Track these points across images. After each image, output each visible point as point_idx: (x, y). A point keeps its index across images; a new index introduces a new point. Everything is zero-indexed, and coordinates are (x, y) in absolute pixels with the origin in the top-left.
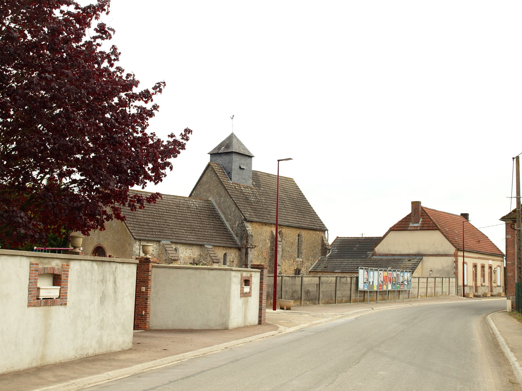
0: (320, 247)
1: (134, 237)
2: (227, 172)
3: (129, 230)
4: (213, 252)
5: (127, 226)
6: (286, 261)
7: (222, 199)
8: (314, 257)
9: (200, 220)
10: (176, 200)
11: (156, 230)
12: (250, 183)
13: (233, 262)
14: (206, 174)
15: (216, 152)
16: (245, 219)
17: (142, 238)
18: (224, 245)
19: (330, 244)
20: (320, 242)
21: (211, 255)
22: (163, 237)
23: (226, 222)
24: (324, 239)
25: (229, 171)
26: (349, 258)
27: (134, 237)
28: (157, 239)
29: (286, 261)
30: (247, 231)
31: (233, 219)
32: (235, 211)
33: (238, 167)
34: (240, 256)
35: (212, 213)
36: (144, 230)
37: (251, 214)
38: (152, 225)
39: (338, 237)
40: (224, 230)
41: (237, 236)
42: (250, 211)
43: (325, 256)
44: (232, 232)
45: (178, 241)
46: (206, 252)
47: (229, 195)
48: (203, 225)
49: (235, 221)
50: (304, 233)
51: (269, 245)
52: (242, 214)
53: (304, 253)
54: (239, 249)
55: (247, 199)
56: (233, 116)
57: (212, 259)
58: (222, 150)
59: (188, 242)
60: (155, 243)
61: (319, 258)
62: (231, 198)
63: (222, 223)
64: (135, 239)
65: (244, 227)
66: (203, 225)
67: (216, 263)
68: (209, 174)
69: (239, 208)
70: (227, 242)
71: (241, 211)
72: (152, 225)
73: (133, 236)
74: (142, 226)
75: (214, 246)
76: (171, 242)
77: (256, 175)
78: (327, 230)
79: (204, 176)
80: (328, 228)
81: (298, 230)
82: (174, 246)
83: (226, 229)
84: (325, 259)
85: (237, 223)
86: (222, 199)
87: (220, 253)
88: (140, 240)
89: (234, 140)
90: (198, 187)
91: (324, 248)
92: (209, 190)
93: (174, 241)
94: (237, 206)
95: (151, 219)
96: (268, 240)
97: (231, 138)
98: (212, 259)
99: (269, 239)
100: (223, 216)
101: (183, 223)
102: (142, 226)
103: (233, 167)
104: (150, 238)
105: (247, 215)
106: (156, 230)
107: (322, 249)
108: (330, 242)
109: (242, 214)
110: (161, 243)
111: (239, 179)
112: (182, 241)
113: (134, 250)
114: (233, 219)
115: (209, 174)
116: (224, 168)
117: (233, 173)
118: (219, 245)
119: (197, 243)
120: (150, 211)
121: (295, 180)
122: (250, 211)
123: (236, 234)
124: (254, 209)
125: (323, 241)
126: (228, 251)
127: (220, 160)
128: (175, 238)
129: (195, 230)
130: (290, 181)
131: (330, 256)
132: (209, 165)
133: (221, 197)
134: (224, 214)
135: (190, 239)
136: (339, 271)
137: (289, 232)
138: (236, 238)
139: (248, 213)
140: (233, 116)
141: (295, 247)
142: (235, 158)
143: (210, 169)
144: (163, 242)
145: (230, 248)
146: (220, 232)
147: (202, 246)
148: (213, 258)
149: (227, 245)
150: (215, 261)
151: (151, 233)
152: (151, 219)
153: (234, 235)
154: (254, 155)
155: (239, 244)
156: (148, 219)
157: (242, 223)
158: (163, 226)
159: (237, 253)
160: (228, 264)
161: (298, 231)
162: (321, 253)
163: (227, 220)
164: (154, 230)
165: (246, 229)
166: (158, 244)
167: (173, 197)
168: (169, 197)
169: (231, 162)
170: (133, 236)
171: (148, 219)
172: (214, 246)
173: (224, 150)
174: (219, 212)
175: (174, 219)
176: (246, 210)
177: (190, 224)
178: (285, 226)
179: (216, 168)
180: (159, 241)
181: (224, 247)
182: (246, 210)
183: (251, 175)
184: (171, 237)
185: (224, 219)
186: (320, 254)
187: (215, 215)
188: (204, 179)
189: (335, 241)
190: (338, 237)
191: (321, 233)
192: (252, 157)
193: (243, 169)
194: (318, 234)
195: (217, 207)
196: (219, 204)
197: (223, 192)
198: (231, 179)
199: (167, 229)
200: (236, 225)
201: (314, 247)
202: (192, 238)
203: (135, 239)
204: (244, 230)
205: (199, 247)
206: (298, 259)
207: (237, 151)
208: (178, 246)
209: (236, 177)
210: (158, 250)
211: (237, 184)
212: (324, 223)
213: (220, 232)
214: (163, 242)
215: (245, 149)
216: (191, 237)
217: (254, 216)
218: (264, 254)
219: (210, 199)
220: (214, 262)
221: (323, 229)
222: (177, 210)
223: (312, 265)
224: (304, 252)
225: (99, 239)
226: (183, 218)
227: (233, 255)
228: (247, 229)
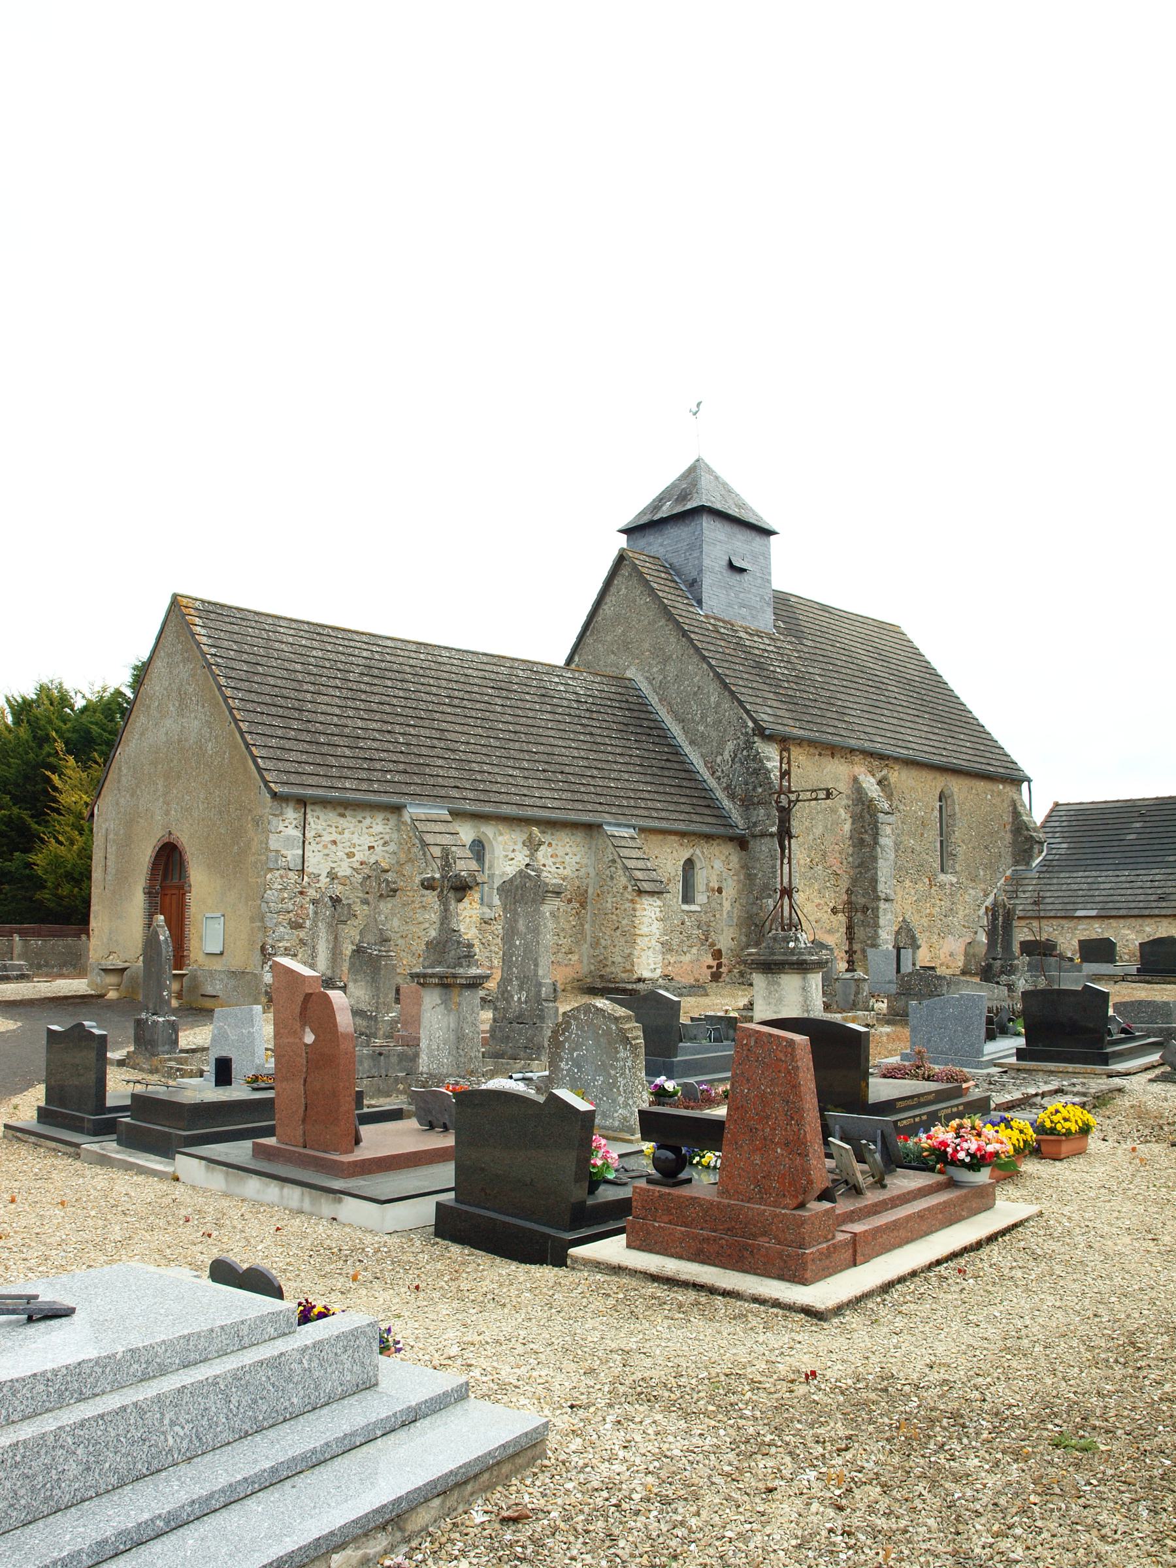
0: (1008, 837)
1: (269, 789)
2: (684, 582)
3: (254, 758)
4: (639, 854)
5: (247, 745)
6: (908, 883)
7: (672, 670)
8: (991, 867)
9: (588, 738)
10: (495, 669)
11: (391, 766)
12: (766, 621)
13: (720, 891)
14: (613, 590)
15: (645, 519)
16: (760, 732)
17: (310, 791)
18: (681, 827)
19: (1038, 824)
20: (1008, 818)
21: (631, 864)
22: (418, 790)
23: (688, 749)
24: (1020, 809)
25: (694, 574)
26: (1117, 867)
27: (269, 789)
28: (384, 798)
29: (908, 883)
30: (768, 771)
31: (714, 734)
32: (718, 705)
33: (725, 563)
34: (745, 867)
35: (638, 720)
36: (332, 761)
37: (779, 713)
38: (375, 745)
39: (1057, 804)
40: (683, 775)
41: (732, 797)
42: (775, 704)
43: (1028, 864)
44: (712, 783)
45: (488, 808)
46: (610, 853)
47: (697, 649)
48: (603, 756)
49: (722, 743)
50: (958, 787)
51: (847, 827)
52: (747, 712)
53: (961, 857)
54: (742, 843)
55: (759, 666)
56: (699, 405)
57: (631, 878)
58: (664, 512)
59: (529, 812)
60: (380, 817)
61: (1009, 873)
62: (704, 658)
63: (676, 751)
64: (274, 795)
65: (757, 758)
66: (603, 756)
67: (652, 893)
68: (623, 591)
69: (732, 693)
70: (695, 818)
71: (740, 703)
72: (375, 745)
73: (266, 783)
74: (325, 749)
75: (642, 830)
76: (451, 813)
77: (784, 604)
78: (1029, 781)
79: (608, 599)
80: (1028, 772)
81: (938, 775)
82: (467, 833)
83: (689, 773)
84: (1030, 875)
85: (730, 746)
86: (672, 670)
87: (668, 859)
88: (302, 803)
89: (705, 481)
90: (589, 640)
91: (1023, 840)
92: (626, 646)
93: (468, 806)
94: (725, 686)
95: (374, 725)
96: (842, 811)
97: (693, 474)
98: (631, 878)
99: (847, 807)
100: (676, 730)
101: (517, 746)
102: (325, 749)
103: (706, 562)
104: (350, 795)
105: (765, 717)
106: (391, 766)
107: (1014, 843)
108: (1038, 815)
109: (747, 712)
110: (406, 817)
111: (730, 605)
112: (506, 810)
113: (274, 844)
114: (714, 734)
115: (623, 591)
116: (670, 570)
117: (707, 582)
118: (664, 825)
119: (573, 816)
120: (377, 699)
121: (904, 629)
122: (775, 704)
123: (728, 787)
124: (790, 701)
125: (1016, 814)
126: (703, 853)
127: (659, 545)
128: (471, 795)
129: (567, 769)
130: (893, 631)
131: (1047, 865)
132: (621, 559)
133: (666, 660)
134: (680, 720)
135: (539, 802)
136: (1094, 913)
137: (911, 783)
138: (727, 803)
139: (769, 711)
140: (699, 405)
141: (932, 835)
142: (709, 528)
143: (625, 572)
144: (414, 811)
145: (708, 837)
146: (666, 781)
147: (591, 829)
148: (639, 875)
149: (693, 827)
150: (646, 886)
151: (364, 775)
152: (374, 725)
153: (720, 794)
154: (777, 530)
155: (741, 823)
156: (360, 723)
157: (749, 745)
158: (424, 751)
159: (735, 859)
160: (701, 898)
161: (939, 782)
162: (1014, 856)
163: (692, 743)
164: (378, 766)
165: (764, 767)
166: (392, 823)
167: (485, 659)
168: (470, 657)
169: (696, 546)
170: (266, 783)
171: (360, 723)
172: (642, 830)
173: (671, 507)
174: (663, 713)
175: (480, 731)
176: (759, 701)
177: (549, 749)
178: (896, 759)
179: (646, 568)
180: (397, 809)
181: (682, 834)
182: (759, 701)
183: (769, 596)
184: (454, 793)
185: (681, 739)
186: (1010, 861)
187: (645, 724)
188: (607, 609)
189: (1049, 816)
190: (1057, 804)
191: (1008, 788)
192: (768, 533)
193: (742, 571)
194: (999, 793)
195: (654, 699)
196: (661, 689)
197: (673, 645)
198: (700, 602)
199: (440, 762)
200: (726, 756)
201: (991, 834)
202: (547, 800)
203: (274, 795)
204: (756, 772)
205: (579, 836)
206: (942, 877)
207: (718, 506)
208: (489, 831)
209: (718, 598)
210: (392, 847)
211: (724, 622)
212: (1014, 757)
213: (666, 781)
214: (414, 811)
215: (742, 505)
216: (547, 794)
217: (791, 723)
218: (831, 860)
219: (629, 674)
220: (640, 892)
221: (1015, 778)
222: (499, 701)
223: (986, 895)
224: (961, 850)
225: (167, 813)
226: (518, 728)
227: (718, 864)
228: (769, 765)
